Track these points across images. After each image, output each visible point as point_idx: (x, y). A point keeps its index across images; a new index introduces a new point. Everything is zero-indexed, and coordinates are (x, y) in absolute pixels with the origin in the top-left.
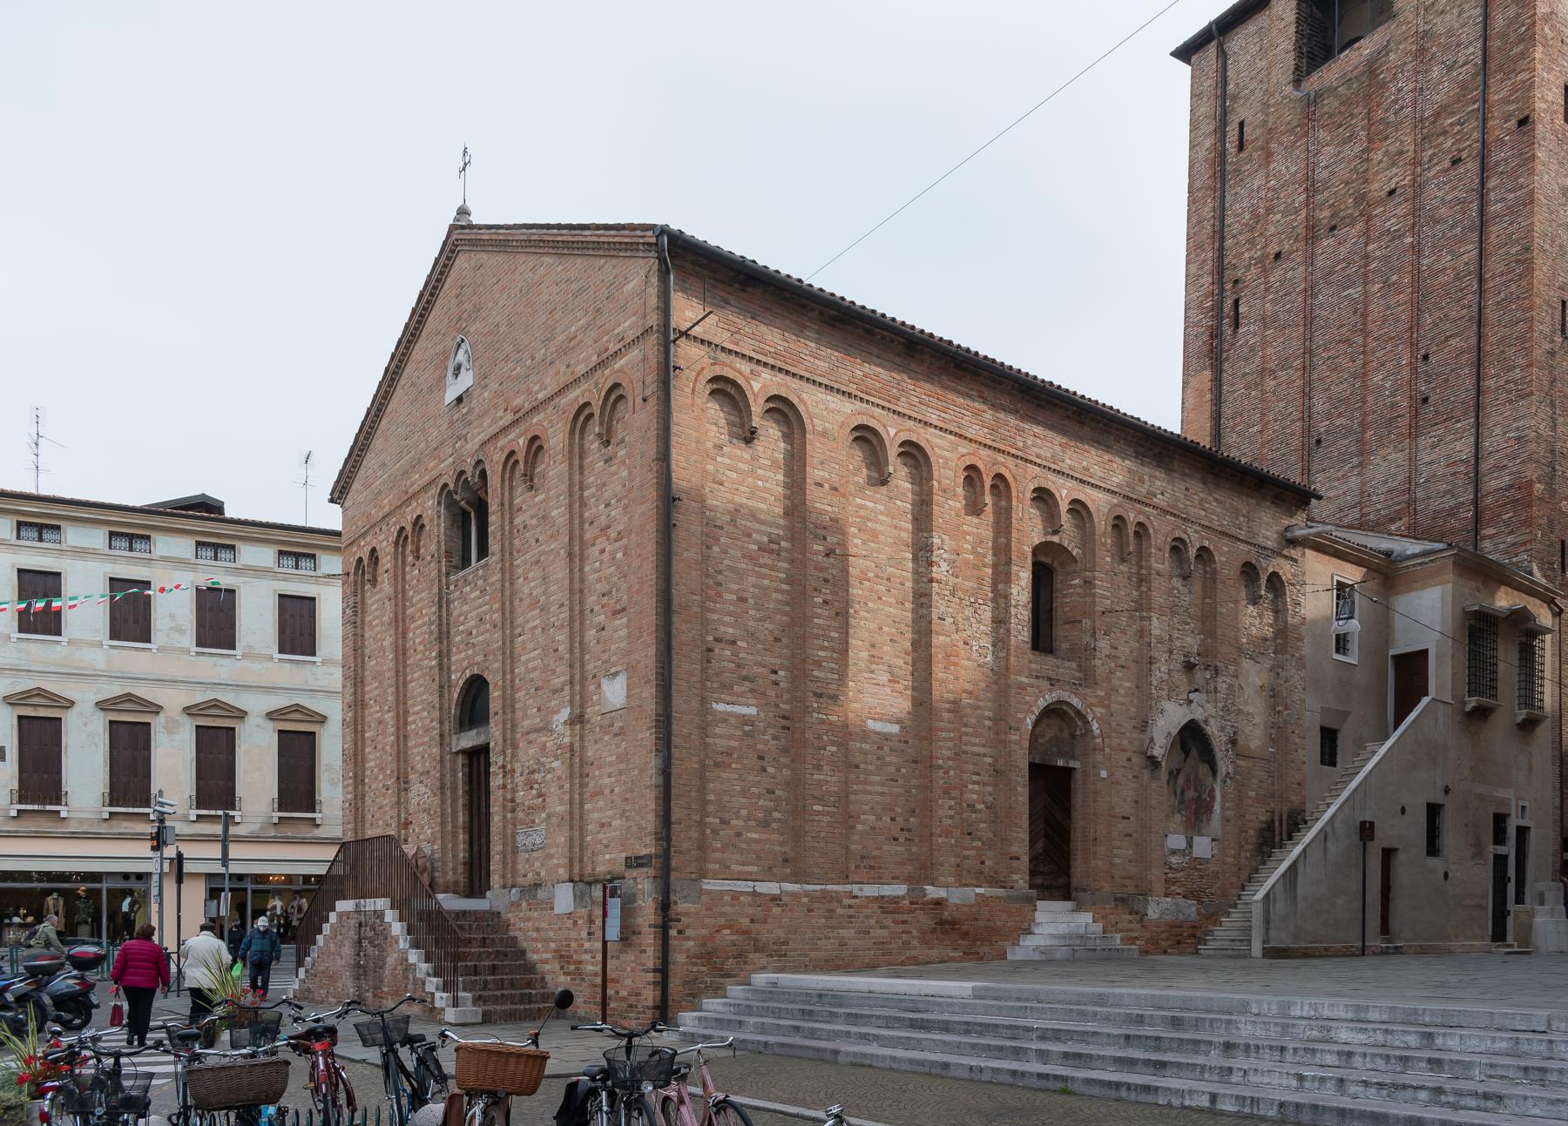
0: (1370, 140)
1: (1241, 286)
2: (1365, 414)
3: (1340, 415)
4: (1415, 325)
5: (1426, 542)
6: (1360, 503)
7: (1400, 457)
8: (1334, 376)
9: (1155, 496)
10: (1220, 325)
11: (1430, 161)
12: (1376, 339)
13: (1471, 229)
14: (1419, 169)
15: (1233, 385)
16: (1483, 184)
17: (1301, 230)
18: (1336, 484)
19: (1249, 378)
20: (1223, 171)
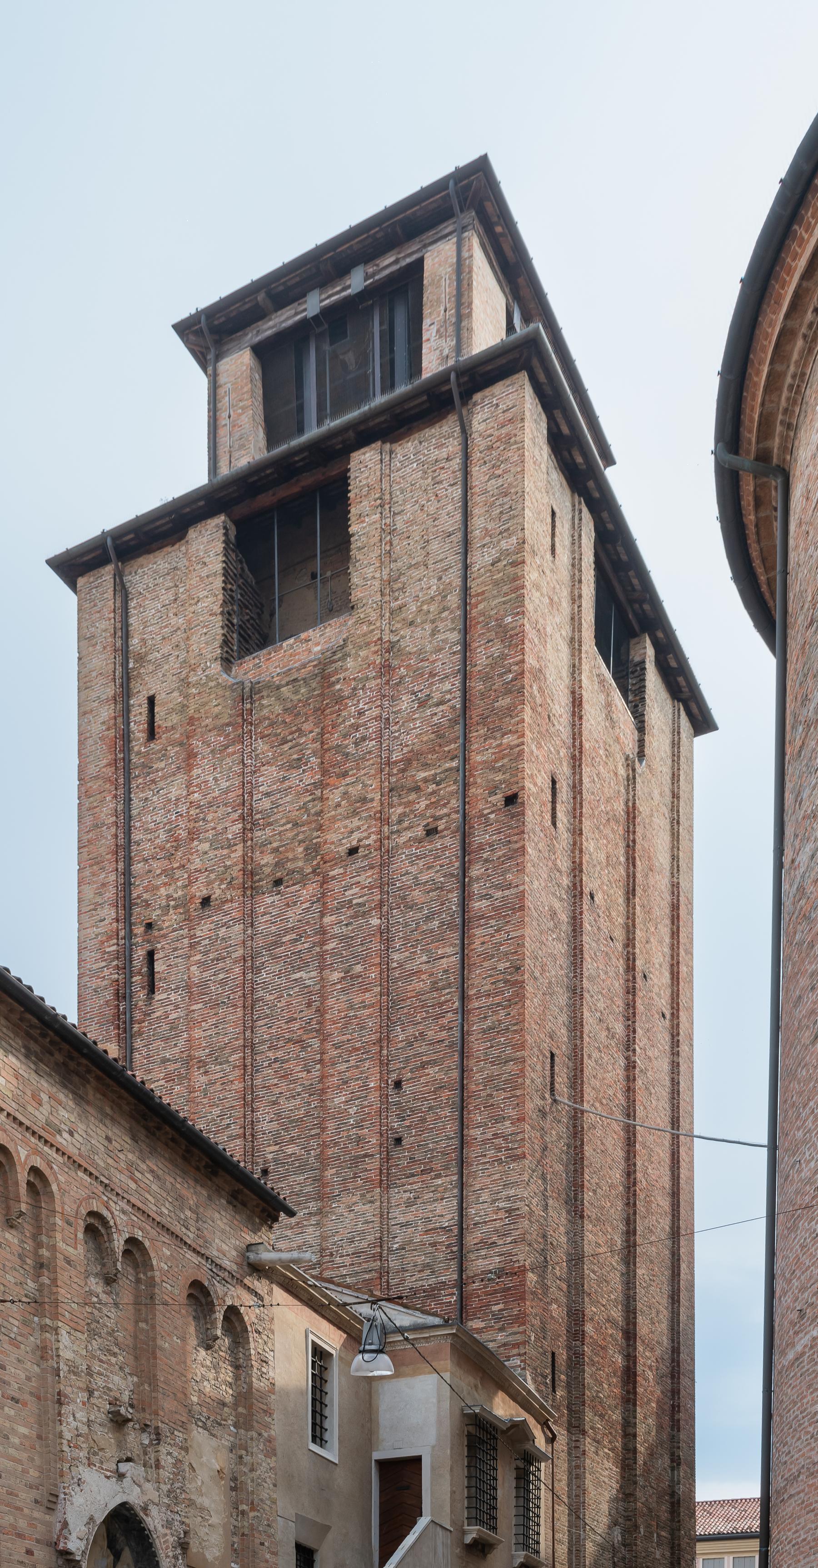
0: (324, 772)
1: (156, 933)
2: (324, 1145)
3: (292, 1141)
4: (384, 1039)
5: (418, 1314)
6: (319, 1263)
7: (370, 1211)
8: (283, 1086)
9: (59, 1132)
10: (128, 983)
11: (400, 822)
12: (336, 1047)
13: (451, 926)
14: (386, 828)
15: (149, 1071)
16: (464, 870)
17: (236, 872)
18: (289, 1233)
19: (171, 1067)
20: (127, 761)
